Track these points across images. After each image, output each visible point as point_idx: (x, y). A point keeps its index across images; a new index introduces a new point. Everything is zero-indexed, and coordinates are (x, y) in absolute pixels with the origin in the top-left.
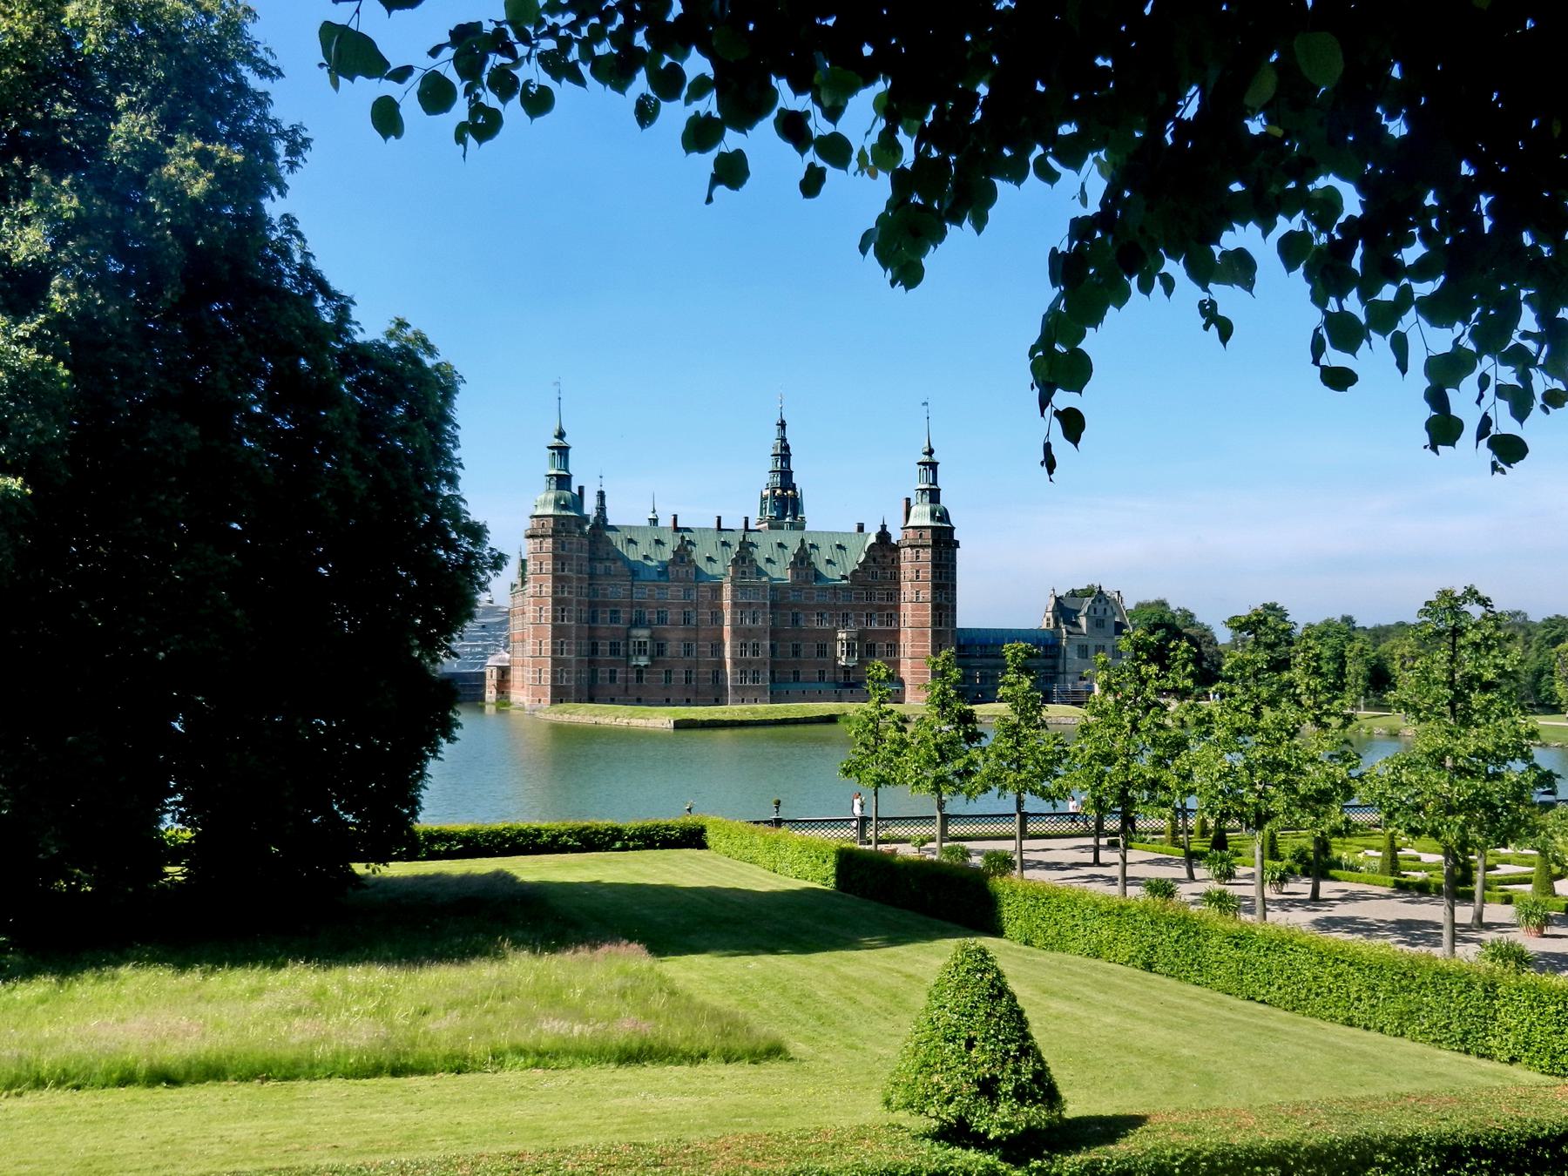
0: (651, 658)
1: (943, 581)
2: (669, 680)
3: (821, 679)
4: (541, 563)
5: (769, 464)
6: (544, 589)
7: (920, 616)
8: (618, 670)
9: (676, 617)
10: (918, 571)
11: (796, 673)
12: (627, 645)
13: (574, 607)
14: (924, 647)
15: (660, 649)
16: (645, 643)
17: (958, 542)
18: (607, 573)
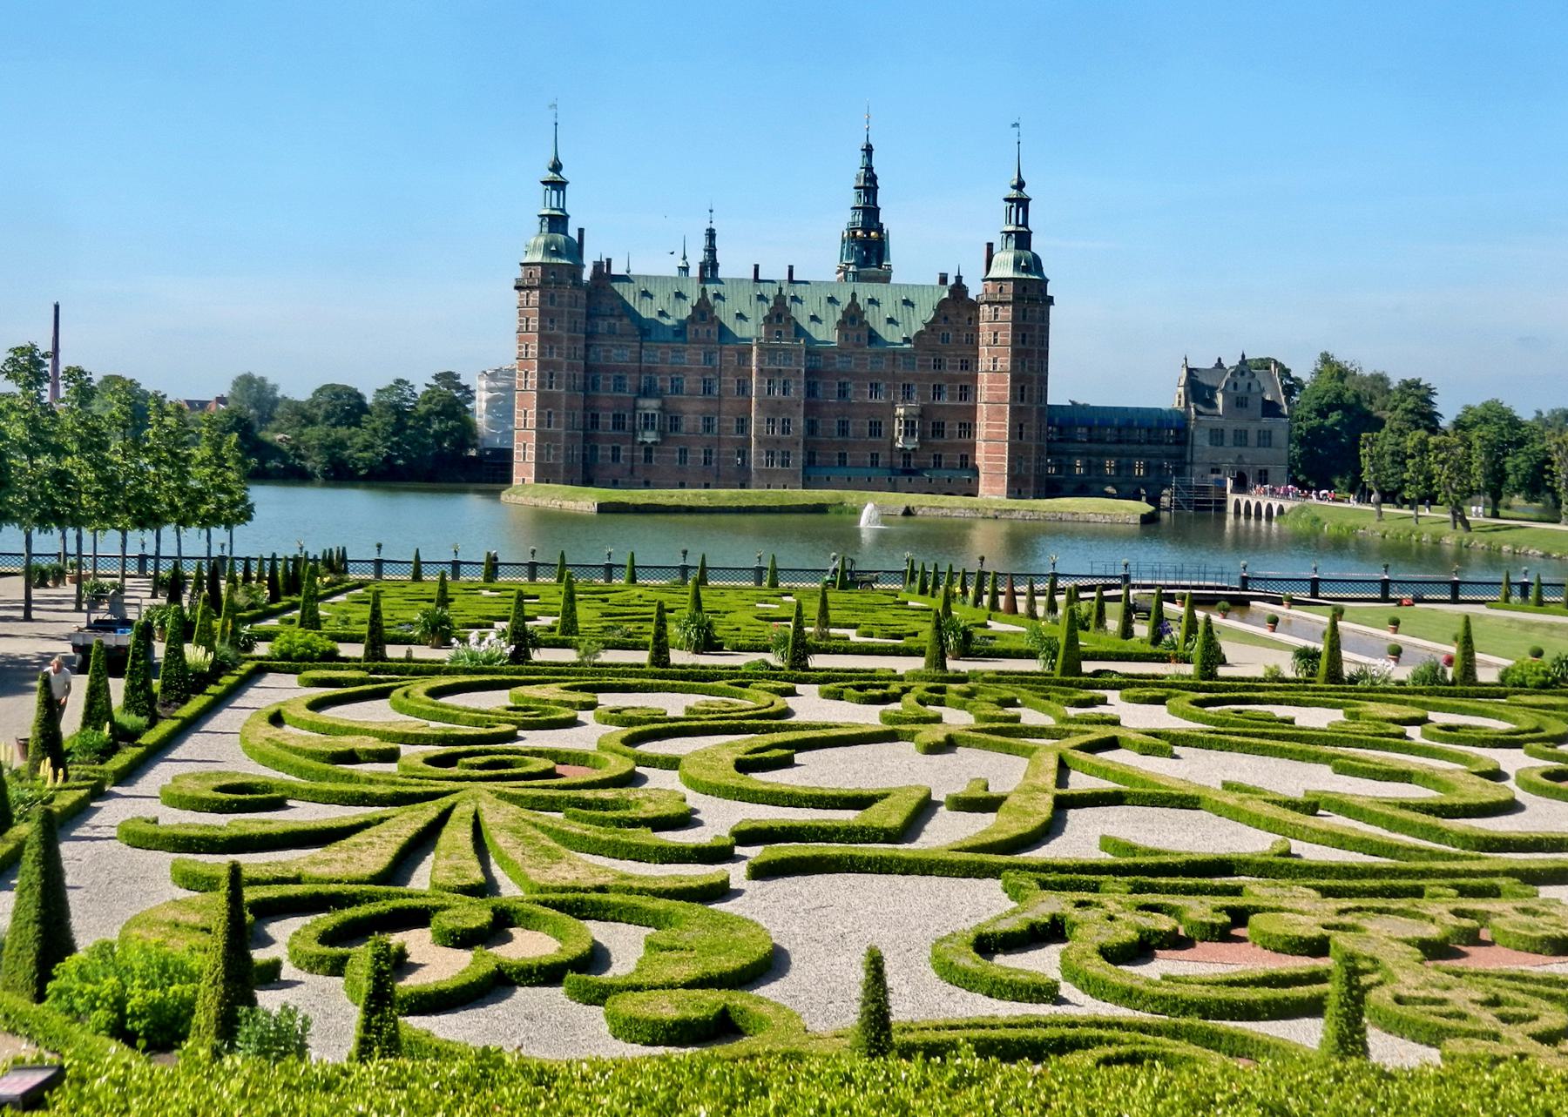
0: (662, 433)
1: (1027, 346)
2: (683, 460)
3: (875, 464)
4: (527, 320)
5: (852, 198)
6: (530, 350)
7: (997, 388)
8: (622, 447)
9: (693, 386)
10: (996, 334)
11: (842, 456)
12: (634, 418)
13: (564, 372)
14: (1000, 427)
15: (675, 424)
16: (653, 415)
17: (1052, 298)
18: (612, 332)
